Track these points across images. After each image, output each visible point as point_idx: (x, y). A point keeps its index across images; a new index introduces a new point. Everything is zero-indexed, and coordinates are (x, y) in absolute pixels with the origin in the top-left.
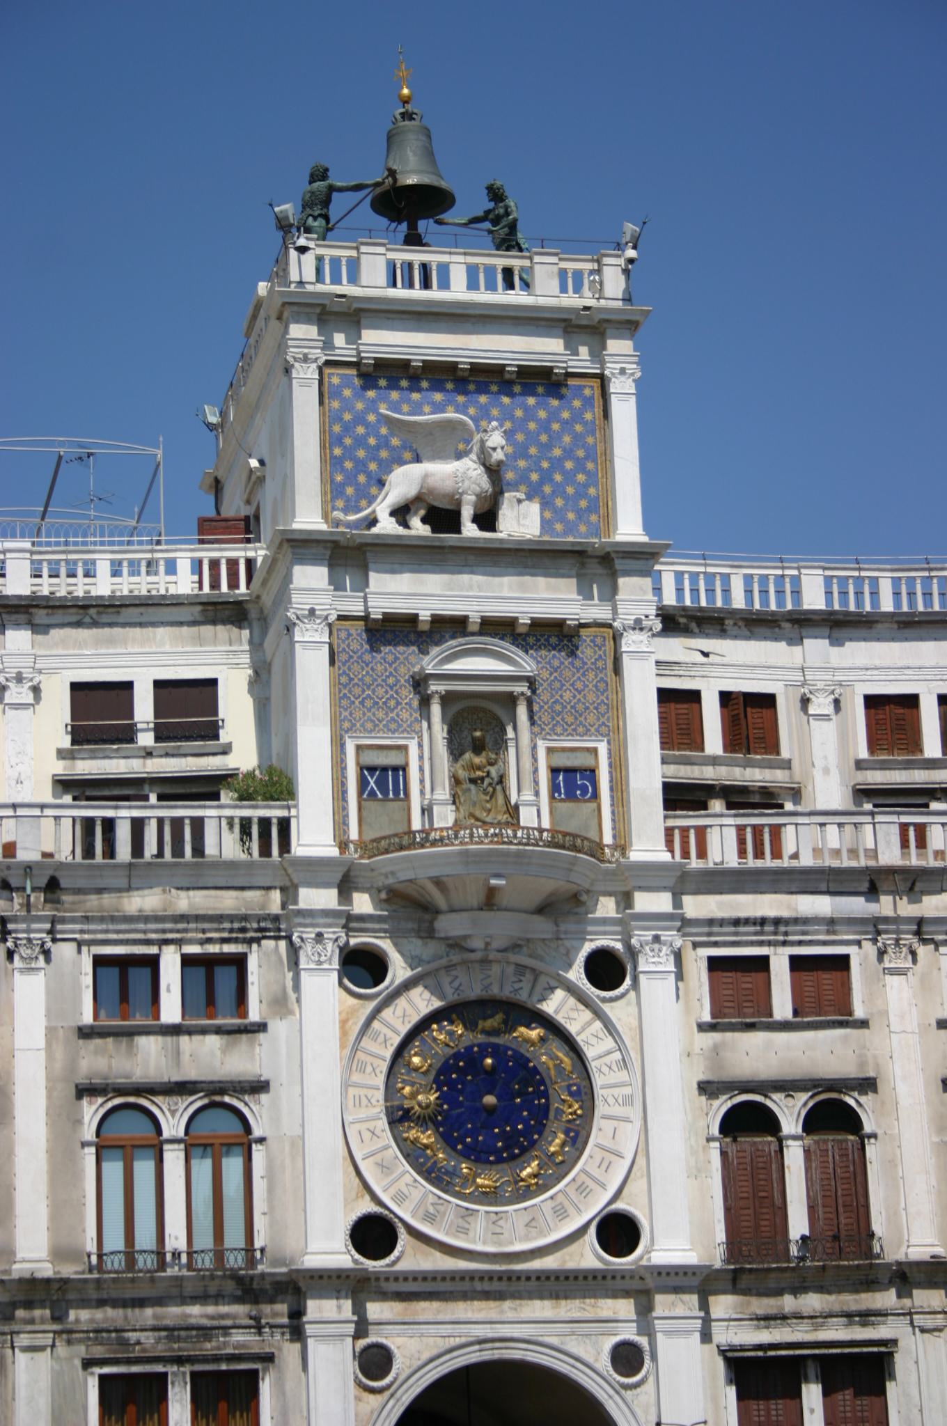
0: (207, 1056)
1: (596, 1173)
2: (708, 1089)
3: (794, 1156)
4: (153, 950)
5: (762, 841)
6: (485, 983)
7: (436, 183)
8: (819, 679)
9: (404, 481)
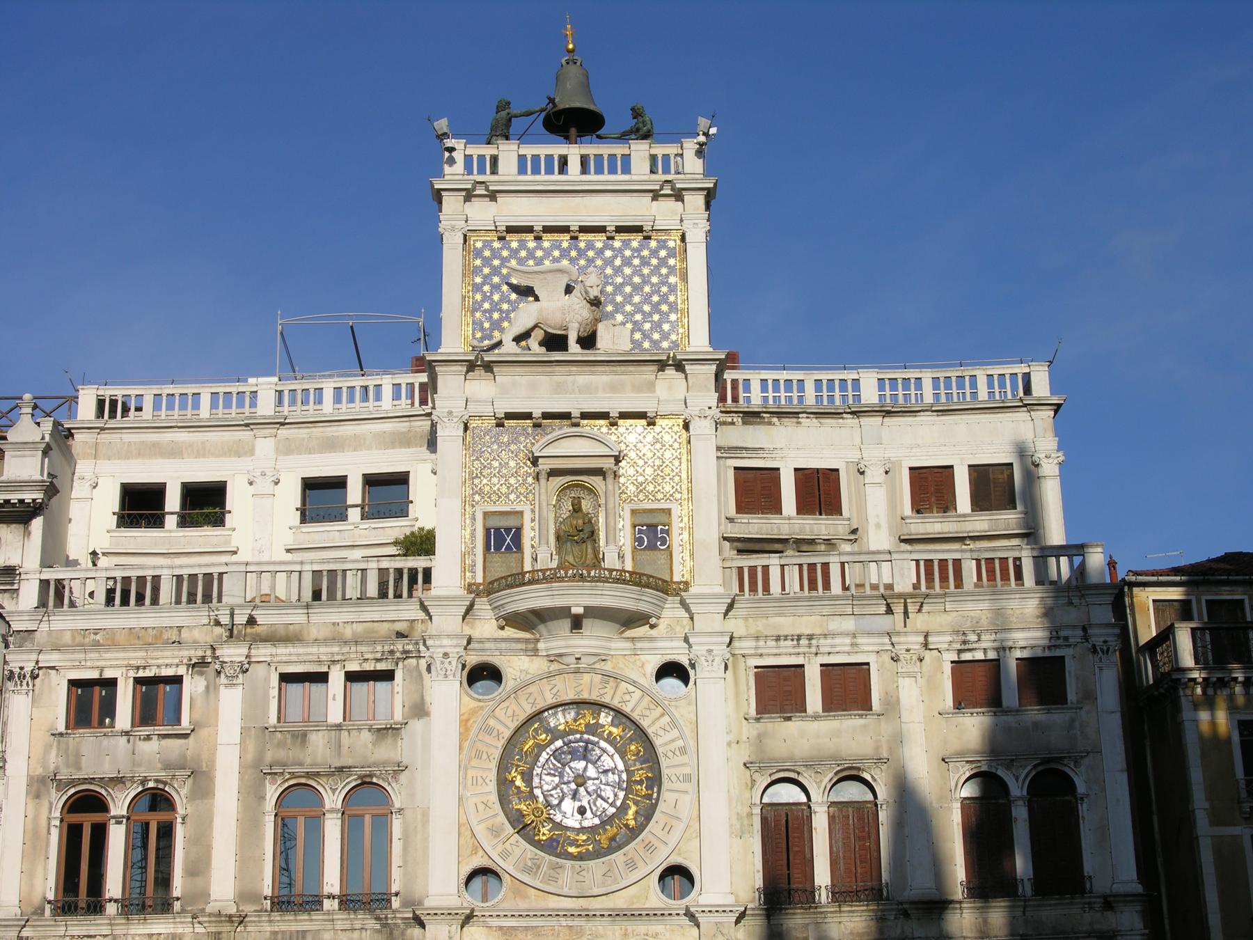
0: (361, 748)
1: (660, 834)
4: (325, 669)
5: (815, 578)
6: (578, 689)
7: (585, 106)
8: (874, 458)
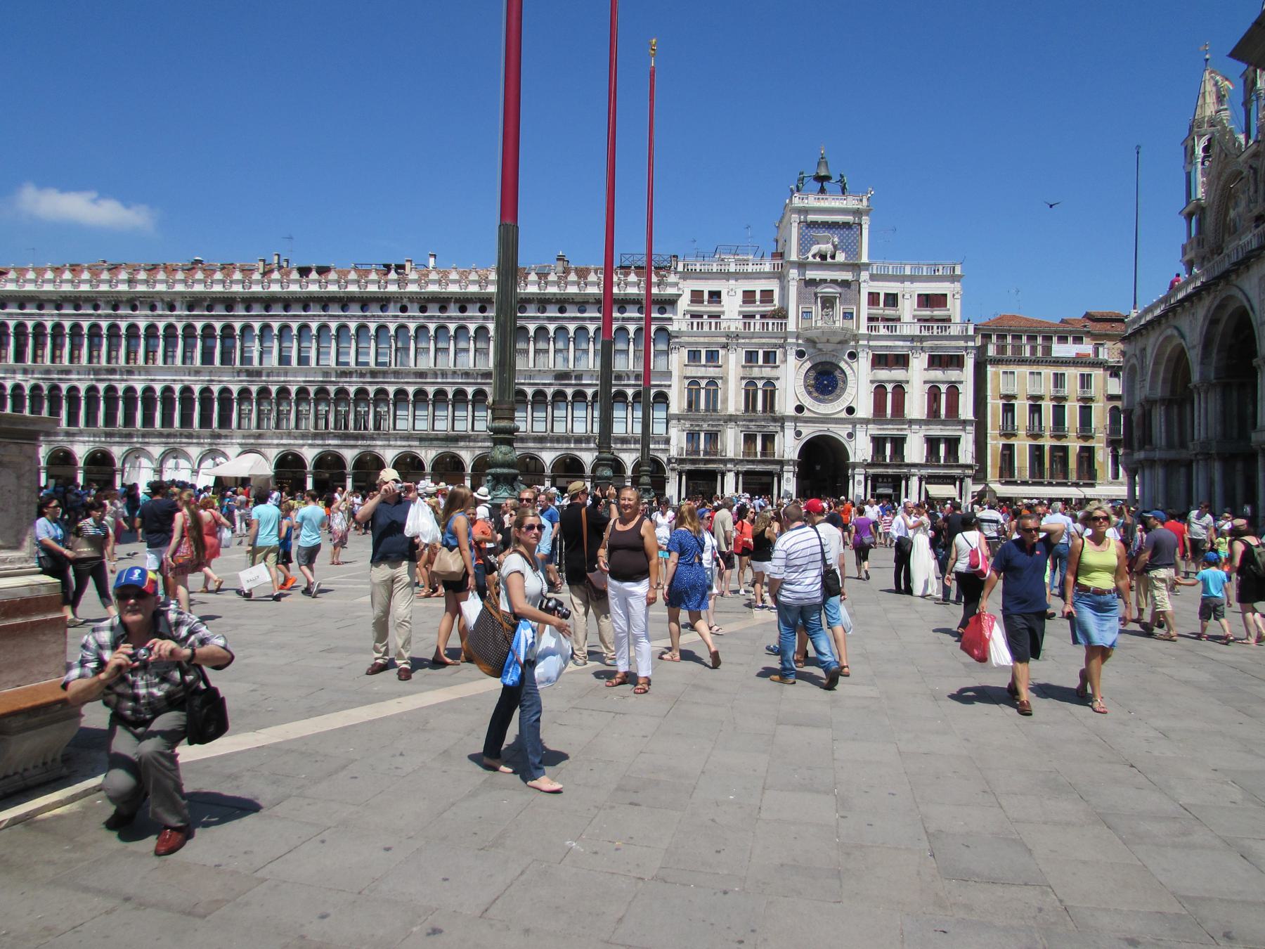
0: (767, 372)
2: (872, 382)
3: (889, 397)
9: (815, 249)
